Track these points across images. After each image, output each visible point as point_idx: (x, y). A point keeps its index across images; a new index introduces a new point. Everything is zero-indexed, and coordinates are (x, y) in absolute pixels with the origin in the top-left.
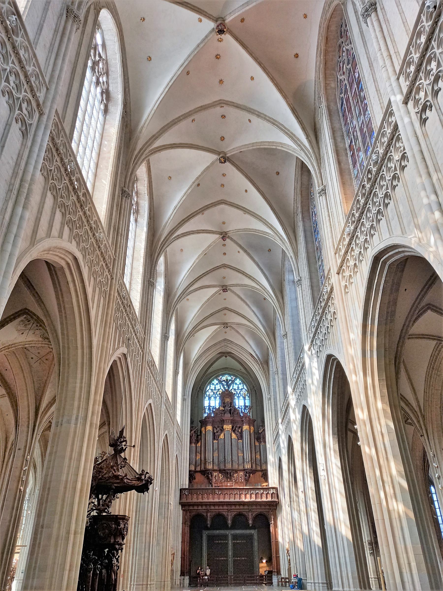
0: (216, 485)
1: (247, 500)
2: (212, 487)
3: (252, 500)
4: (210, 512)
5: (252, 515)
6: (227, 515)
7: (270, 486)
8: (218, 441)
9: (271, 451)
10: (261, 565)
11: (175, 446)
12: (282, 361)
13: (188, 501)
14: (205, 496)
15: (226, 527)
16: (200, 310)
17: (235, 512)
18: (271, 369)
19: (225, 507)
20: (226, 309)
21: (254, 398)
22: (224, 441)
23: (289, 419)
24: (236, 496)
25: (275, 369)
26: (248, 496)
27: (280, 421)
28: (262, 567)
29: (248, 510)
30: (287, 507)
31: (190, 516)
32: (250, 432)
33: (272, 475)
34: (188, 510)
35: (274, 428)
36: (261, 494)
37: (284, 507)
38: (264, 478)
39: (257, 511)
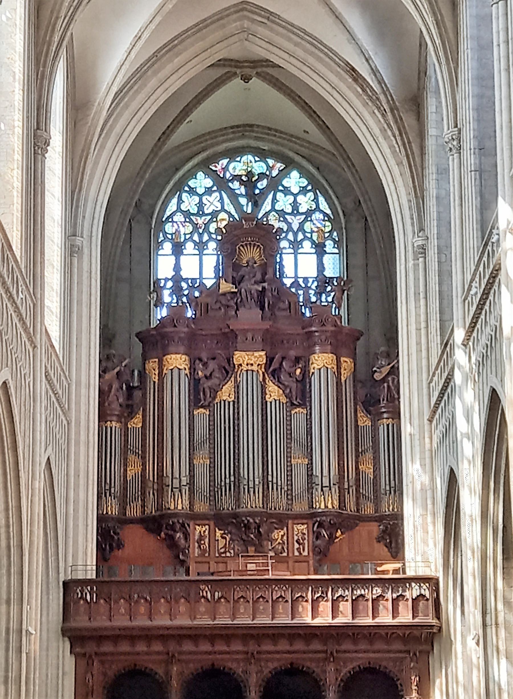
0: (204, 568)
1: (318, 621)
2: (188, 573)
3: (340, 620)
7: (410, 573)
9: (417, 449)
11: (41, 427)
12: (480, 97)
14: (162, 606)
17: (272, 660)
18: (432, 131)
19: (237, 646)
21: (358, 248)
23: (498, 329)
24: (280, 607)
25: (448, 132)
26: (326, 606)
27: (459, 335)
29: (324, 655)
30: (471, 643)
31: (105, 674)
32: (339, 378)
33: (420, 534)
35: (434, 361)
36: (375, 601)
37: (458, 646)
38: (388, 546)
39: (352, 660)
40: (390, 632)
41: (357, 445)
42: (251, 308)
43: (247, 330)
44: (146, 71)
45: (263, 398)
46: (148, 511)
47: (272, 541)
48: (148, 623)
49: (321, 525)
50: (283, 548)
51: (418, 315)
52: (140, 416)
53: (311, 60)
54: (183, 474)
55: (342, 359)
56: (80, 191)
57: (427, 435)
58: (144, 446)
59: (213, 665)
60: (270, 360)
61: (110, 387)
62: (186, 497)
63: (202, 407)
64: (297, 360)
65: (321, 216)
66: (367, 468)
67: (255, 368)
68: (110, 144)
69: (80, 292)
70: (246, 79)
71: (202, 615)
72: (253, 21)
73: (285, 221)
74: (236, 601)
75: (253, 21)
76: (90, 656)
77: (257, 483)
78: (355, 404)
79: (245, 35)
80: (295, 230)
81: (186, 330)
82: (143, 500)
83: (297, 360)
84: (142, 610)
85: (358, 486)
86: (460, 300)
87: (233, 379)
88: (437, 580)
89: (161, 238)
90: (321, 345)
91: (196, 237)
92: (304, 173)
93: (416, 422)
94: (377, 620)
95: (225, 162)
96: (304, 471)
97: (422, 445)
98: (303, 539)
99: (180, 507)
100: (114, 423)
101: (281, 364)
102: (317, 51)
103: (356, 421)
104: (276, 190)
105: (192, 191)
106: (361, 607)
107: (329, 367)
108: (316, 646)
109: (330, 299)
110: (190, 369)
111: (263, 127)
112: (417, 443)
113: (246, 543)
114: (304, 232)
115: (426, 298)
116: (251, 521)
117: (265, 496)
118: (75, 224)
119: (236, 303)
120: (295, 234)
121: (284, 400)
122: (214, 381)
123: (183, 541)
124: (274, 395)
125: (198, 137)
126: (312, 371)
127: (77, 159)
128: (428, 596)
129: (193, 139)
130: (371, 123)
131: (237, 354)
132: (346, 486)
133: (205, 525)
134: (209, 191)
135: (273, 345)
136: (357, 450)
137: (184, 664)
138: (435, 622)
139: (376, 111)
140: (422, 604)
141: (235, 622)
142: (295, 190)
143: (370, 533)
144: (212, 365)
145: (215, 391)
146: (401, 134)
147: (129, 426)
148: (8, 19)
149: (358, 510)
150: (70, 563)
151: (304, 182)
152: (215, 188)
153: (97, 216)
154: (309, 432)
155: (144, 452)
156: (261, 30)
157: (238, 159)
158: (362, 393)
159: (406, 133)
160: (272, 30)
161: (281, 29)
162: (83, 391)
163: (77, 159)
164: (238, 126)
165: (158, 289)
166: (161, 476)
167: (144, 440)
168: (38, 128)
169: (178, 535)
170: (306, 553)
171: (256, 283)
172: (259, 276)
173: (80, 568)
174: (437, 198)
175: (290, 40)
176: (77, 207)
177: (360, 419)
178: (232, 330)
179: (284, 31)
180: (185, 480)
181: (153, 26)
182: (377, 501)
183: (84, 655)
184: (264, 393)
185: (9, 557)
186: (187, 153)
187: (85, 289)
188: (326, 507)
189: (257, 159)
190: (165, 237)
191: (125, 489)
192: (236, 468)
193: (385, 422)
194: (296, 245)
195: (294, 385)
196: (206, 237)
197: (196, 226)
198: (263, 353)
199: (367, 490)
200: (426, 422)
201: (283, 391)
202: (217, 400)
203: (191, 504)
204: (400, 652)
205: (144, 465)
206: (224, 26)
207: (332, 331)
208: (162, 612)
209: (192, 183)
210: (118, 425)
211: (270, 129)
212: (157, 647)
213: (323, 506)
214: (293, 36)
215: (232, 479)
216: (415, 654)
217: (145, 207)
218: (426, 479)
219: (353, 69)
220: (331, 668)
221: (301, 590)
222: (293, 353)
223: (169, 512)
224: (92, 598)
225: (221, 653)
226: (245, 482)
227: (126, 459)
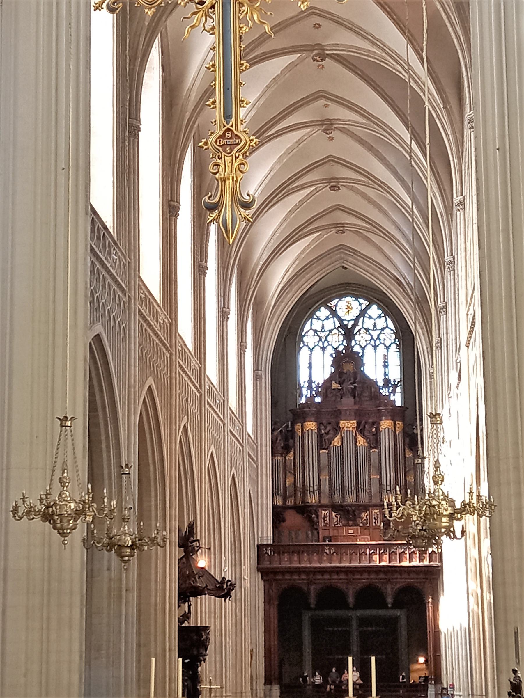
5: (392, 588)
6: (347, 588)
8: (329, 451)
15: (345, 605)
22: (342, 450)
29: (385, 580)
31: (278, 590)
41: (405, 467)
42: (349, 397)
45: (356, 444)
46: (297, 503)
48: (298, 565)
50: (367, 522)
52: (292, 453)
54: (315, 484)
55: (397, 422)
60: (359, 424)
61: (277, 439)
63: (324, 449)
64: (373, 423)
65: (389, 331)
67: (351, 429)
73: (370, 334)
75: (346, 254)
77: (353, 488)
78: (404, 445)
79: (342, 260)
80: (375, 339)
81: (314, 409)
83: (373, 423)
84: (296, 559)
87: (340, 434)
89: (302, 345)
90: (386, 416)
91: (321, 344)
92: (380, 307)
95: (336, 301)
99: (314, 501)
100: (279, 458)
101: (365, 427)
103: (405, 454)
104: (364, 317)
105: (318, 318)
107: (390, 427)
110: (317, 429)
111: (357, 284)
113: (348, 520)
114: (380, 340)
116: (350, 509)
117: (357, 496)
119: (341, 394)
120: (375, 341)
121: (366, 444)
122: (330, 436)
123: (315, 519)
124: (362, 443)
125: (321, 291)
126: (381, 429)
127: (258, 331)
128: (436, 552)
130: (407, 306)
131: (342, 422)
133: (326, 510)
134: (327, 318)
135: (360, 415)
138: (440, 564)
139: (410, 301)
141: (341, 565)
142: (375, 316)
147: (287, 458)
150: (260, 535)
151: (380, 312)
152: (331, 316)
154: (380, 462)
155: (295, 472)
156: (350, 259)
157: (343, 299)
158: (407, 440)
159: (425, 314)
162: (264, 449)
163: (258, 331)
164: (343, 284)
165: (301, 388)
166: (304, 485)
169: (313, 516)
170: (379, 525)
171: (351, 384)
173: (265, 538)
175: (365, 264)
177: (407, 453)
178: (339, 410)
180: (316, 488)
183: (268, 580)
184: (356, 442)
186: (316, 299)
187: (263, 397)
189: (354, 299)
190: (304, 345)
192: (343, 481)
194: (375, 347)
196: (326, 344)
198: (355, 422)
201: (366, 440)
202: (332, 445)
206: (331, 258)
207: (391, 409)
208: (305, 560)
209: (318, 313)
210: (281, 458)
211: (360, 285)
215: (340, 486)
219: (398, 279)
220: (389, 587)
222: (370, 421)
223: (308, 504)
226: (347, 489)
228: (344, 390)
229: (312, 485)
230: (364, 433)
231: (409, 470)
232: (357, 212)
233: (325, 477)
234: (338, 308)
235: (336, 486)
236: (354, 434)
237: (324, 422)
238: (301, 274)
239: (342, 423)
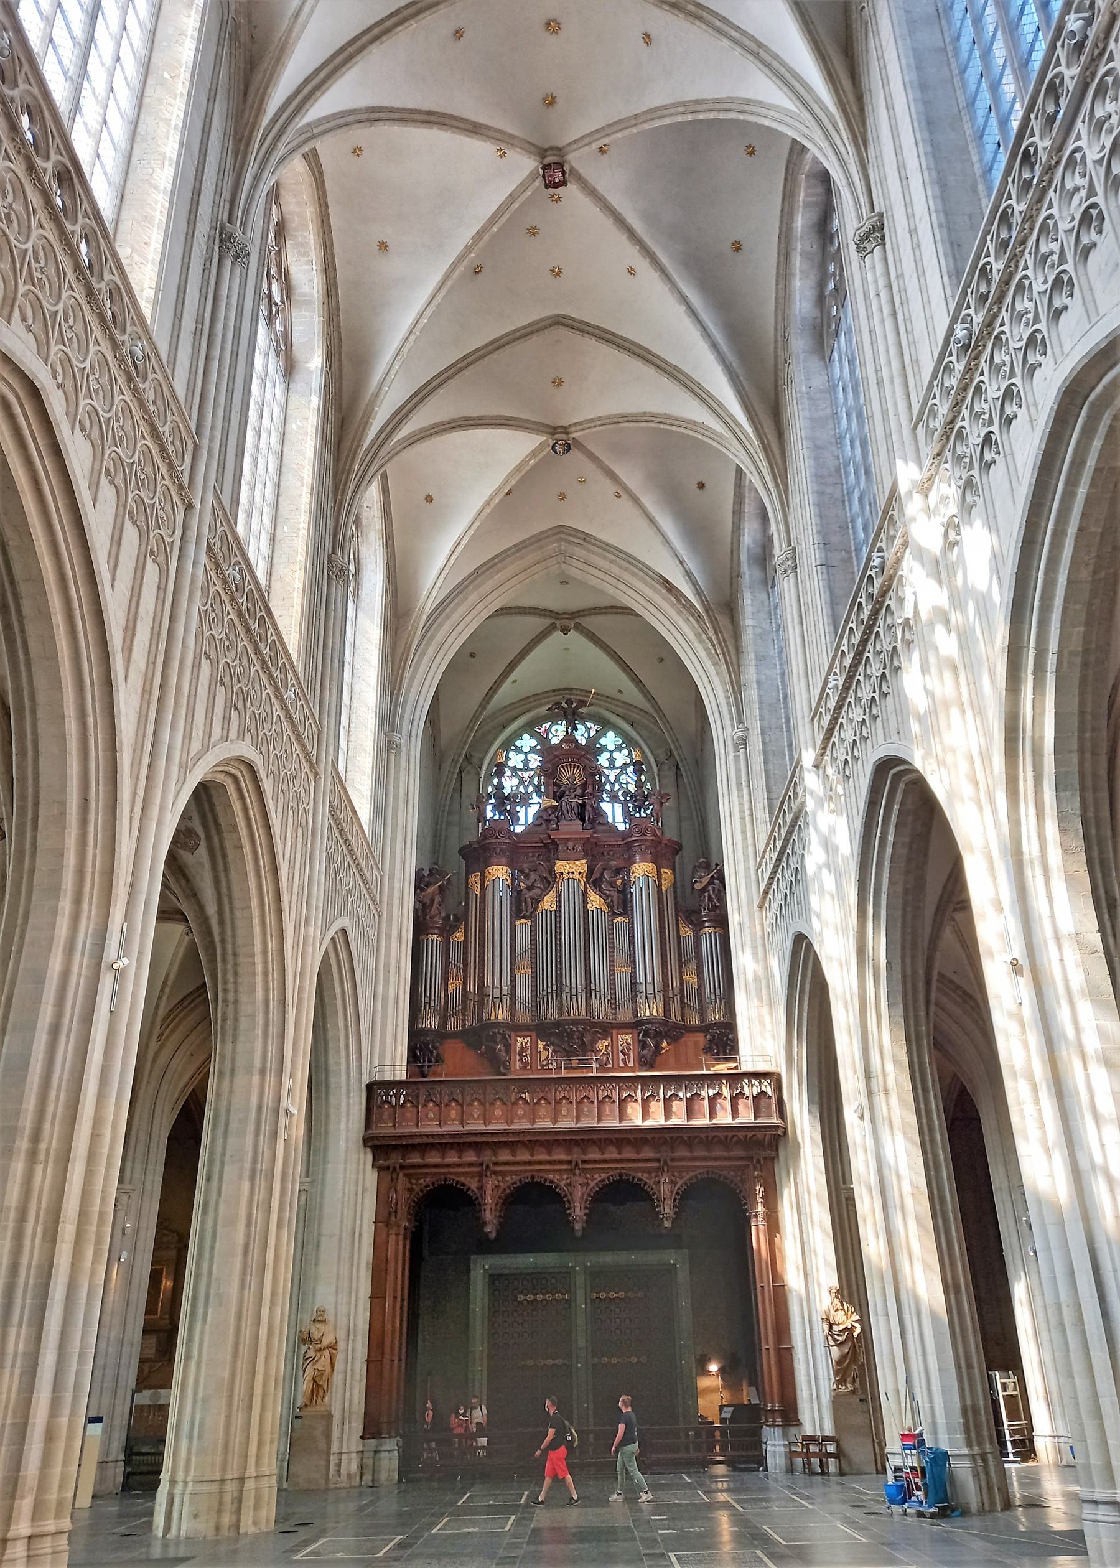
1: (649, 1123)
3: (674, 1122)
4: (495, 1173)
10: (703, 1383)
13: (399, 1131)
16: (443, 292)
19: (560, 1155)
20: (559, 321)
24: (607, 1108)
26: (657, 1107)
28: (708, 1390)
29: (656, 1165)
31: (410, 1190)
34: (402, 1167)
36: (712, 1100)
39: (688, 1169)
40: (730, 1134)
41: (680, 955)
43: (569, 840)
44: (467, 587)
45: (585, 907)
47: (596, 1052)
49: (646, 1034)
51: (741, 804)
52: (462, 930)
53: (627, 577)
55: (663, 870)
56: (400, 689)
57: (757, 922)
58: (465, 960)
59: (533, 1177)
60: (591, 871)
61: (432, 901)
62: (507, 1007)
63: (523, 917)
64: (618, 871)
66: (691, 978)
67: (576, 876)
68: (431, 651)
69: (397, 787)
70: (565, 630)
71: (520, 1119)
72: (570, 542)
74: (558, 1103)
75: (570, 542)
76: (395, 1169)
82: (464, 1014)
83: (618, 871)
85: (682, 997)
86: (807, 719)
88: (779, 1075)
90: (642, 853)
92: (619, 732)
93: (745, 910)
94: (714, 1121)
95: (548, 725)
96: (627, 980)
97: (753, 934)
98: (629, 1049)
99: (500, 1018)
100: (435, 937)
101: (602, 875)
102: (631, 567)
103: (678, 932)
105: (518, 750)
106: (696, 1107)
108: (648, 1153)
109: (649, 812)
112: (747, 932)
115: (749, 786)
117: (588, 1004)
118: (394, 721)
120: (612, 785)
122: (538, 891)
128: (769, 1093)
129: (519, 701)
131: (559, 863)
132: (671, 995)
136: (680, 960)
137: (500, 1178)
138: (779, 1122)
139: (690, 618)
140: (763, 1102)
142: (611, 747)
143: (696, 1044)
144: (533, 876)
145: (537, 901)
146: (716, 634)
148: (299, 428)
149: (683, 1020)
153: (417, 717)
155: (465, 965)
156: (579, 552)
160: (588, 550)
161: (596, 549)
162: (397, 885)
164: (559, 690)
166: (482, 987)
167: (465, 953)
168: (333, 553)
170: (631, 1064)
172: (579, 791)
174: (758, 682)
175: (605, 558)
176: (396, 706)
179: (600, 551)
181: (471, 532)
182: (702, 1012)
183: (388, 1168)
184: (585, 903)
185: (267, 1013)
186: (514, 713)
188: (651, 1014)
191: (446, 1003)
192: (559, 976)
193: (709, 933)
195: (615, 895)
197: (522, 780)
198: (584, 862)
199: (692, 999)
200: (756, 908)
203: (513, 1016)
204: (742, 1158)
205: (465, 978)
206: (542, 547)
209: (518, 743)
210: (440, 939)
212: (470, 1157)
213: (648, 1014)
214: (608, 554)
216: (758, 1161)
217: (475, 760)
218: (760, 969)
219: (667, 581)
220: (665, 1178)
221: (629, 1088)
224: (398, 1100)
225: (540, 1163)
226: (568, 990)
227: (447, 972)
228: (564, 808)
229: (497, 984)
230: (600, 887)
231: (687, 962)
232: (598, 328)
233: (524, 971)
234: (550, 736)
235: (546, 984)
236: (582, 887)
237: (526, 866)
238: (484, 572)
239: (560, 866)
